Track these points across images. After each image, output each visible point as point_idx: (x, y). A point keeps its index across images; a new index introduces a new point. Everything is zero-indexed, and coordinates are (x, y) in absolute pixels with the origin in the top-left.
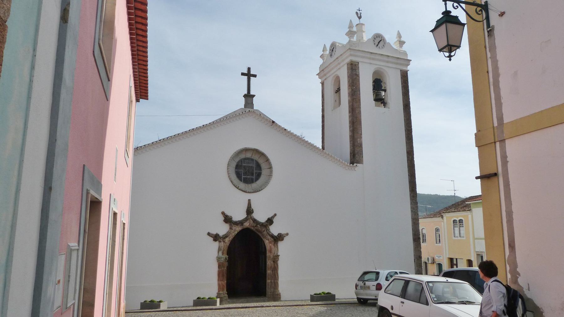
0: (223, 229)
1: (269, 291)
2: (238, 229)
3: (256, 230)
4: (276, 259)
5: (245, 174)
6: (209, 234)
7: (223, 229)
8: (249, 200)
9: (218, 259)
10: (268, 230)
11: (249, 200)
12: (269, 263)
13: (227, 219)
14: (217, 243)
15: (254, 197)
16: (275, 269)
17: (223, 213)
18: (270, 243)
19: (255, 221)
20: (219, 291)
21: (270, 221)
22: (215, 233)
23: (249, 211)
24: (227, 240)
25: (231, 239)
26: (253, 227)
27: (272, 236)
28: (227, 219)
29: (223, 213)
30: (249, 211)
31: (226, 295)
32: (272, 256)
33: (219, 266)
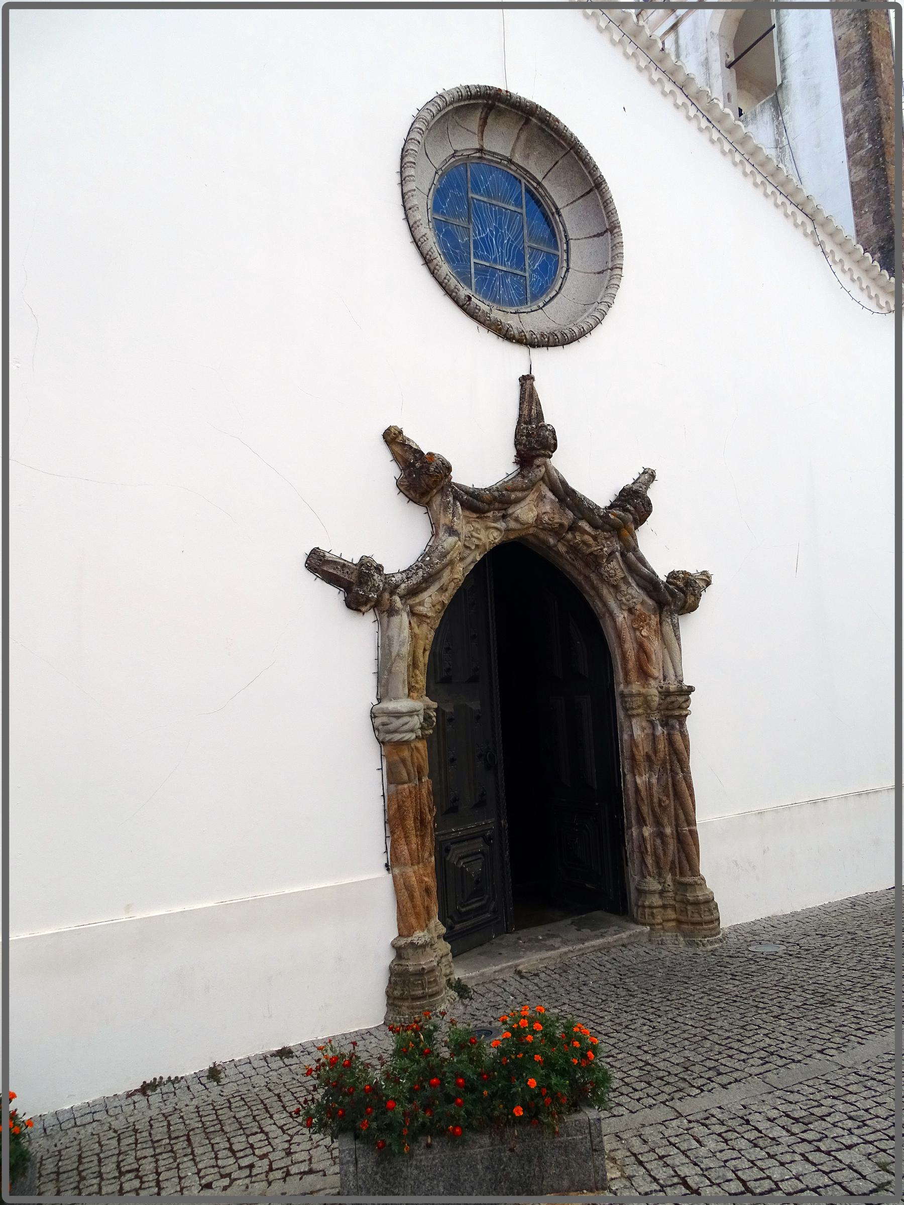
0: (395, 538)
1: (651, 886)
2: (490, 535)
3: (574, 549)
4: (675, 703)
5: (483, 246)
6: (319, 564)
7: (395, 538)
8: (526, 381)
9: (383, 726)
10: (630, 548)
11: (526, 381)
12: (637, 731)
13: (422, 477)
14: (364, 628)
15: (548, 366)
16: (674, 760)
17: (393, 438)
18: (638, 620)
19: (566, 496)
20: (405, 928)
21: (634, 503)
22: (352, 556)
23: (534, 441)
24: (430, 601)
25: (446, 598)
26: (558, 531)
27: (649, 583)
28: (422, 477)
29: (393, 438)
30: (534, 441)
31: (444, 947)
32: (653, 691)
33: (392, 776)
